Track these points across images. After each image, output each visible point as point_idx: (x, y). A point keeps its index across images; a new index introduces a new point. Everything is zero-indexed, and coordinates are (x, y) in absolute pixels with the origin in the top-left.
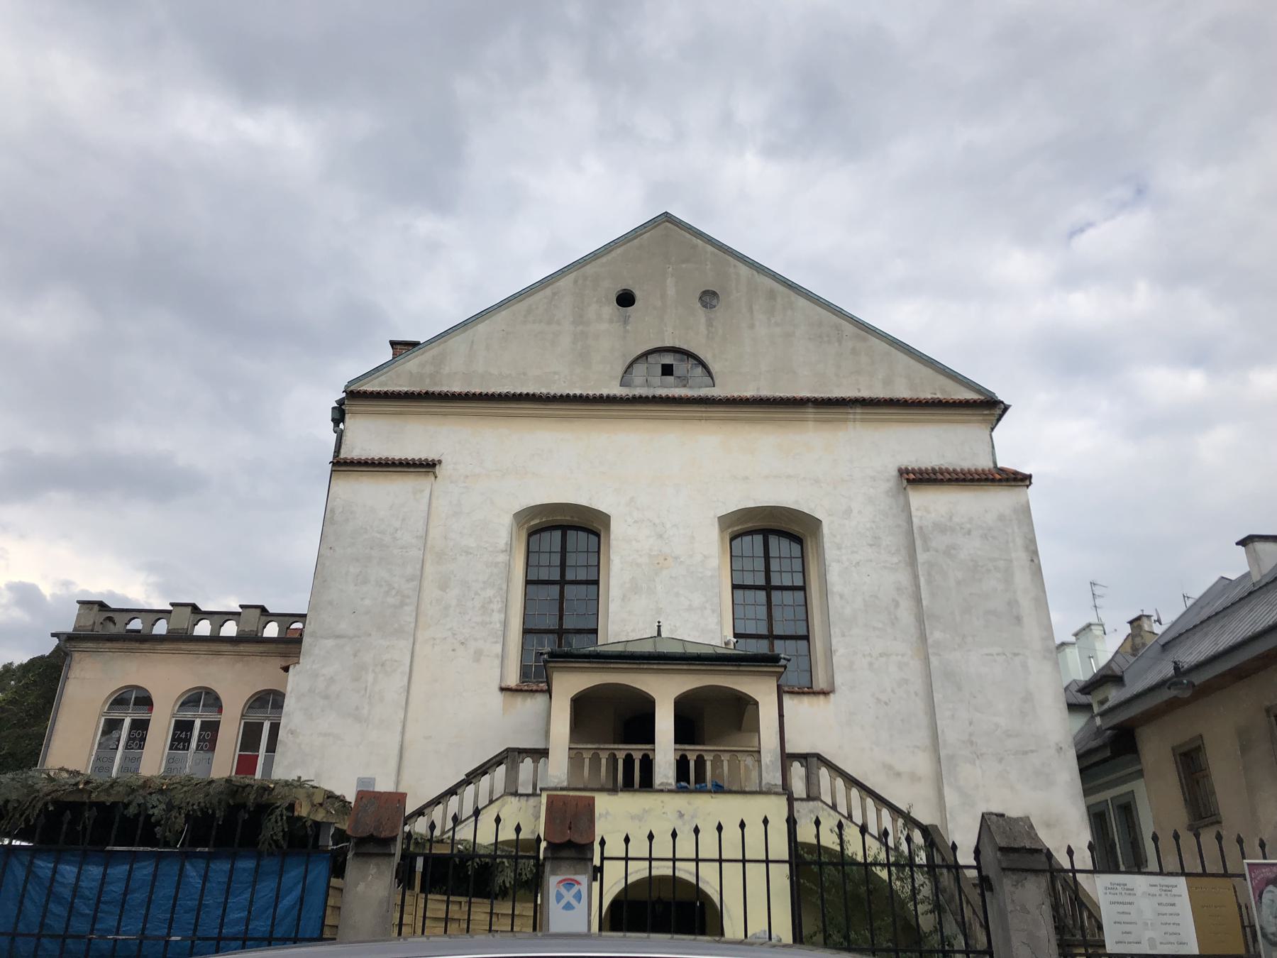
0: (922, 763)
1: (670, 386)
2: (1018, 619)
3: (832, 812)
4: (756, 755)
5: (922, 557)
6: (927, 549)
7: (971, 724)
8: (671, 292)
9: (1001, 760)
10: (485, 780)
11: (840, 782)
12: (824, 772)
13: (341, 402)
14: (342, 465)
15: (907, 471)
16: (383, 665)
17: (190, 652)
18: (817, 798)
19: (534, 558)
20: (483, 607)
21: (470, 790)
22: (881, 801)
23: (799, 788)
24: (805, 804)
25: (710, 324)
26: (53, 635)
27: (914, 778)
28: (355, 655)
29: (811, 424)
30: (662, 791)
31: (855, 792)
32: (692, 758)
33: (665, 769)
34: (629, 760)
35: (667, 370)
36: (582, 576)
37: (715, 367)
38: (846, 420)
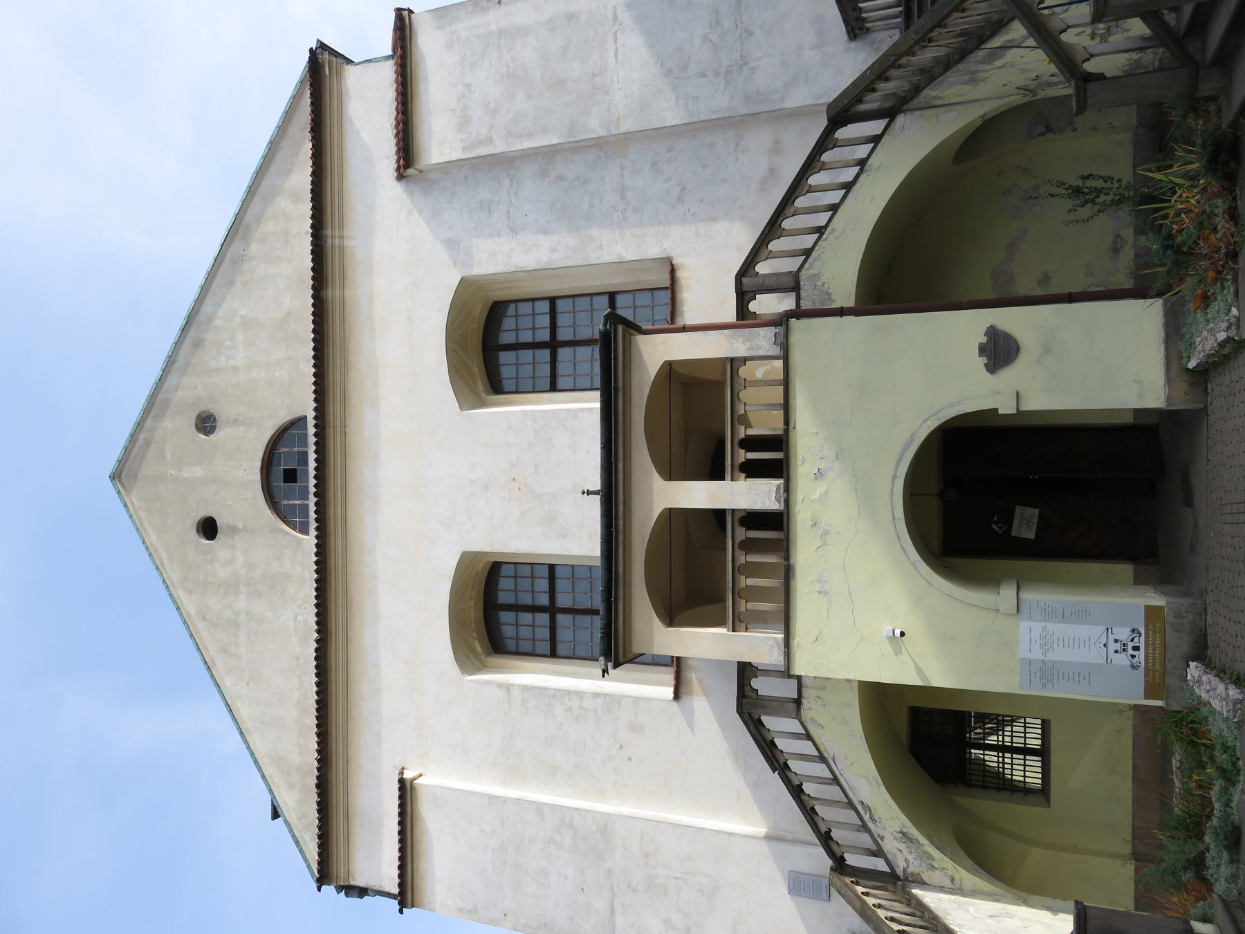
0: (758, 139)
1: (303, 473)
2: (571, 17)
3: (814, 254)
4: (736, 364)
5: (500, 147)
6: (490, 140)
7: (703, 75)
8: (198, 472)
9: (750, 33)
10: (781, 743)
11: (774, 246)
12: (763, 268)
13: (340, 889)
14: (405, 896)
15: (398, 169)
16: (647, 855)
18: (796, 276)
20: (576, 720)
21: (794, 765)
22: (797, 186)
23: (784, 303)
24: (803, 294)
25: (235, 422)
27: (776, 149)
28: (635, 890)
29: (348, 293)
30: (787, 502)
31: (787, 224)
32: (743, 455)
33: (755, 494)
34: (749, 546)
35: (290, 476)
36: (543, 585)
37: (284, 417)
38: (342, 248)
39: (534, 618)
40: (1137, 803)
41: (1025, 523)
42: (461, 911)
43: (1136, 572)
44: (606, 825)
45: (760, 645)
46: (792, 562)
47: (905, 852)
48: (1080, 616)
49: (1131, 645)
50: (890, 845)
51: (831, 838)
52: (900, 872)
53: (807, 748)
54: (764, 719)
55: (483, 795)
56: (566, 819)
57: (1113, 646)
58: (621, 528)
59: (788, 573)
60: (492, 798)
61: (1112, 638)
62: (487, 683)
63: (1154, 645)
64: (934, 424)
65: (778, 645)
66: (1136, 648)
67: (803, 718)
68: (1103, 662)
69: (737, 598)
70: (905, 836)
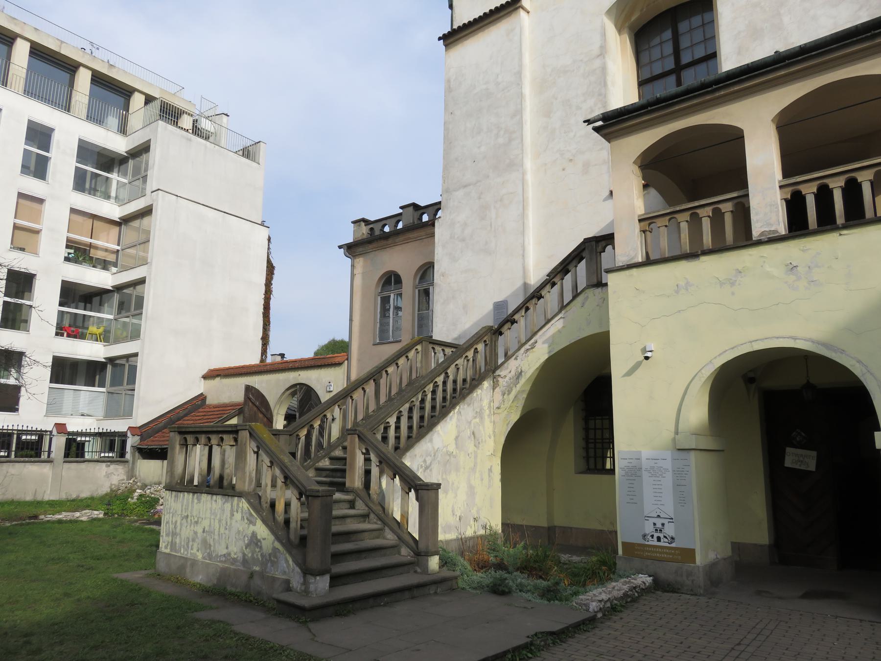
16: (501, 200)
17: (416, 239)
19: (645, 59)
26: (340, 247)
28: (480, 198)
30: (759, 243)
32: (809, 192)
34: (717, 218)
36: (700, 53)
39: (670, 55)
40: (587, 532)
41: (800, 459)
42: (449, 81)
43: (761, 546)
44: (515, 165)
45: (629, 245)
46: (703, 258)
47: (510, 375)
48: (681, 499)
49: (661, 535)
50: (512, 364)
51: (512, 324)
52: (498, 372)
53: (568, 297)
54: (584, 262)
55: (521, 65)
56: (514, 135)
57: (659, 522)
58: (717, 94)
59: (692, 256)
60: (519, 74)
61: (666, 521)
62: (604, 35)
63: (664, 553)
64: (857, 370)
65: (632, 258)
66: (659, 539)
67: (587, 291)
68: (645, 514)
69: (668, 218)
70: (520, 374)
